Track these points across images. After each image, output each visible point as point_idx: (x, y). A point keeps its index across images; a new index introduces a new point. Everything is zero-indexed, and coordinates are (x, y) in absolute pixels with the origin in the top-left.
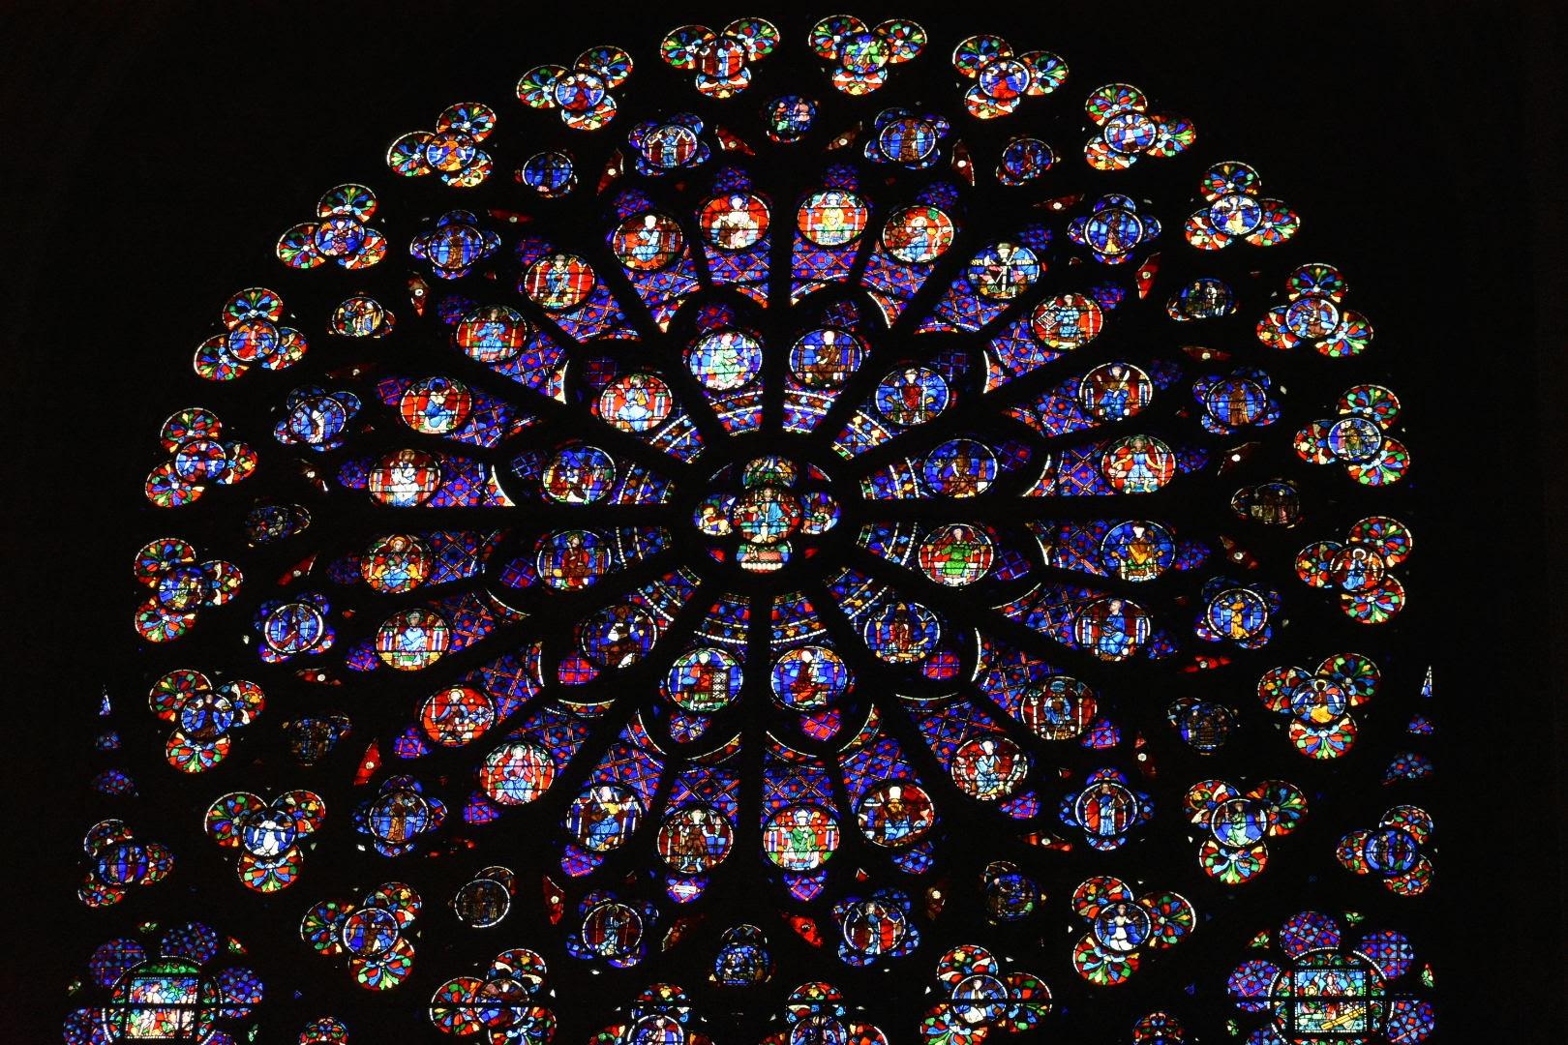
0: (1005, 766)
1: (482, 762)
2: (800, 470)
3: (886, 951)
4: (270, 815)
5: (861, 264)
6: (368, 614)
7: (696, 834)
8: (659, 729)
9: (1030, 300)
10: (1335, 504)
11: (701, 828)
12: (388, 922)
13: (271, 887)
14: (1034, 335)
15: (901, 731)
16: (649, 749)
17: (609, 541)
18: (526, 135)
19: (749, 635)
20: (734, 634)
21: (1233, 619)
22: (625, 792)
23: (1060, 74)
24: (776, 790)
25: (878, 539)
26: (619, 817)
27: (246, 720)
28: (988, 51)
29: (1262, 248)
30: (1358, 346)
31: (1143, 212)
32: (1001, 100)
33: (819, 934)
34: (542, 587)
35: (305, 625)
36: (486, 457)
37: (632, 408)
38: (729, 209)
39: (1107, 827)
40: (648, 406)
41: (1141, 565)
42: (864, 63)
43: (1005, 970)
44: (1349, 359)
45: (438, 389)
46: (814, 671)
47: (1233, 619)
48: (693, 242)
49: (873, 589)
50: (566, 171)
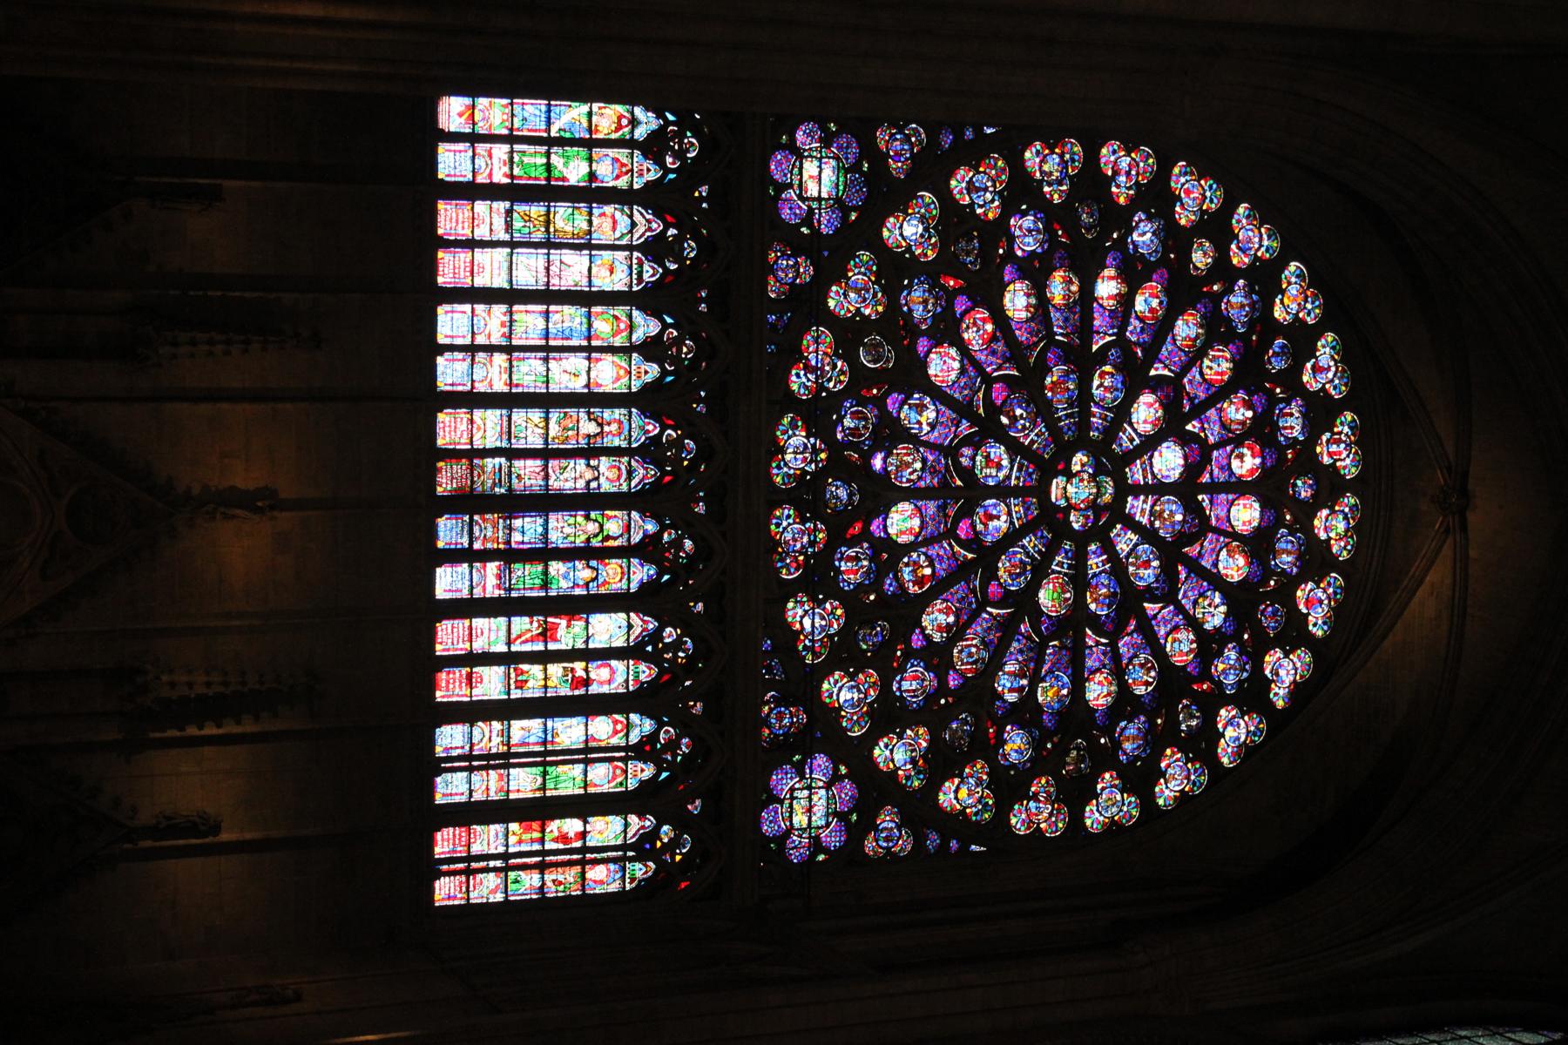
0: (940, 629)
1: (951, 345)
2: (1107, 506)
3: (841, 573)
4: (926, 229)
5: (1219, 531)
6: (1035, 272)
7: (908, 465)
8: (967, 441)
9: (1194, 624)
10: (1075, 794)
11: (908, 466)
12: (864, 300)
13: (886, 234)
14: (1176, 629)
15: (960, 571)
16: (956, 436)
17: (1071, 406)
18: (1302, 339)
19: (1016, 486)
20: (1018, 478)
21: (1015, 744)
22: (933, 426)
23: (1320, 633)
24: (931, 507)
25: (1066, 552)
26: (919, 423)
27: (979, 211)
28: (1335, 593)
29: (1217, 745)
30: (1161, 802)
31: (1240, 683)
32: (1308, 603)
33: (853, 536)
34: (1050, 370)
35: (1029, 240)
36: (1121, 334)
37: (1145, 412)
38: (1253, 456)
39: (906, 685)
40: (1145, 422)
41: (1046, 695)
42: (1332, 526)
43: (830, 637)
44: (1153, 796)
45: (1161, 303)
46: (995, 523)
47: (1015, 744)
48: (1234, 439)
49: (1039, 552)
50: (1278, 365)
